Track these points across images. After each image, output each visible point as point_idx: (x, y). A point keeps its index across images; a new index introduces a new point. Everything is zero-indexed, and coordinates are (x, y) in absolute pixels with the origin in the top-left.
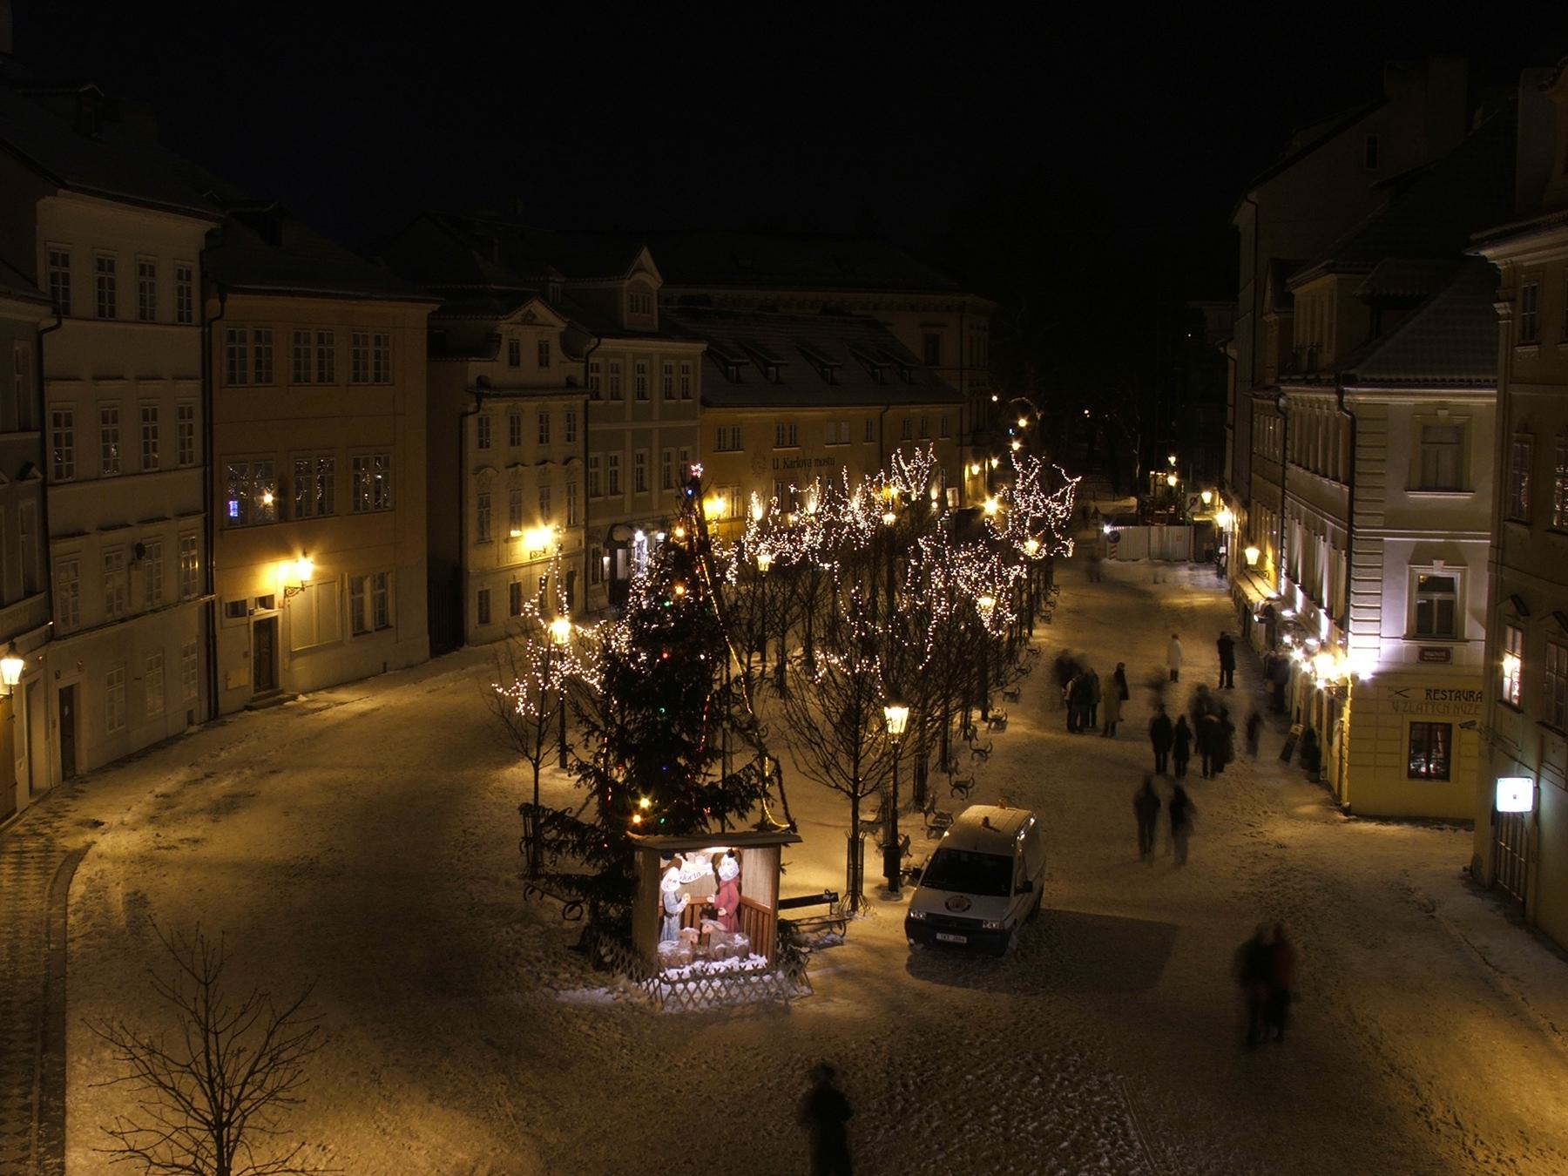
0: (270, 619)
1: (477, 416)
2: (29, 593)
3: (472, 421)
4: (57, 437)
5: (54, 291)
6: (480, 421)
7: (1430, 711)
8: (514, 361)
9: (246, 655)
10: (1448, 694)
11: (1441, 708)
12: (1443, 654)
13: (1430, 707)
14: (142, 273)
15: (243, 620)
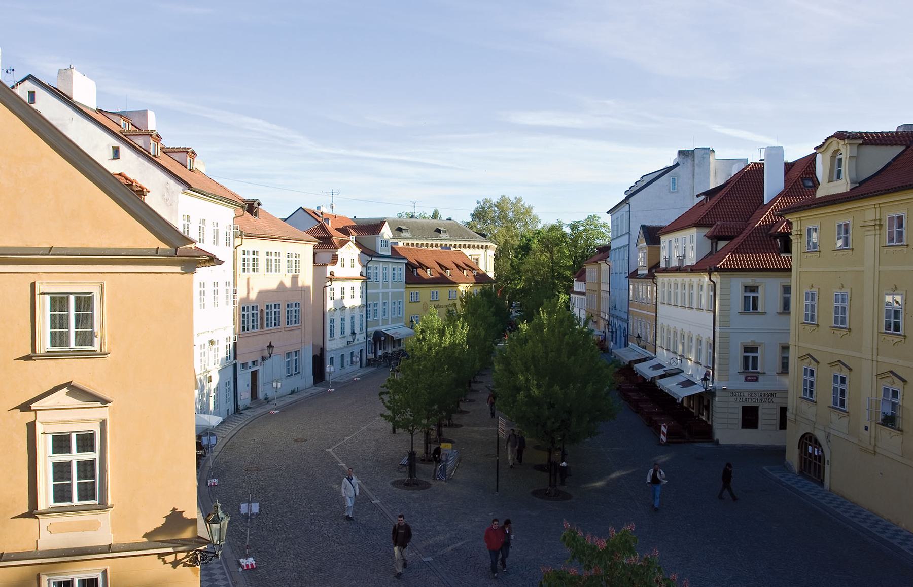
0: (256, 370)
1: (330, 287)
3: (328, 289)
7: (750, 401)
8: (343, 265)
9: (248, 385)
10: (757, 394)
11: (754, 400)
12: (755, 378)
13: (750, 400)
15: (247, 371)
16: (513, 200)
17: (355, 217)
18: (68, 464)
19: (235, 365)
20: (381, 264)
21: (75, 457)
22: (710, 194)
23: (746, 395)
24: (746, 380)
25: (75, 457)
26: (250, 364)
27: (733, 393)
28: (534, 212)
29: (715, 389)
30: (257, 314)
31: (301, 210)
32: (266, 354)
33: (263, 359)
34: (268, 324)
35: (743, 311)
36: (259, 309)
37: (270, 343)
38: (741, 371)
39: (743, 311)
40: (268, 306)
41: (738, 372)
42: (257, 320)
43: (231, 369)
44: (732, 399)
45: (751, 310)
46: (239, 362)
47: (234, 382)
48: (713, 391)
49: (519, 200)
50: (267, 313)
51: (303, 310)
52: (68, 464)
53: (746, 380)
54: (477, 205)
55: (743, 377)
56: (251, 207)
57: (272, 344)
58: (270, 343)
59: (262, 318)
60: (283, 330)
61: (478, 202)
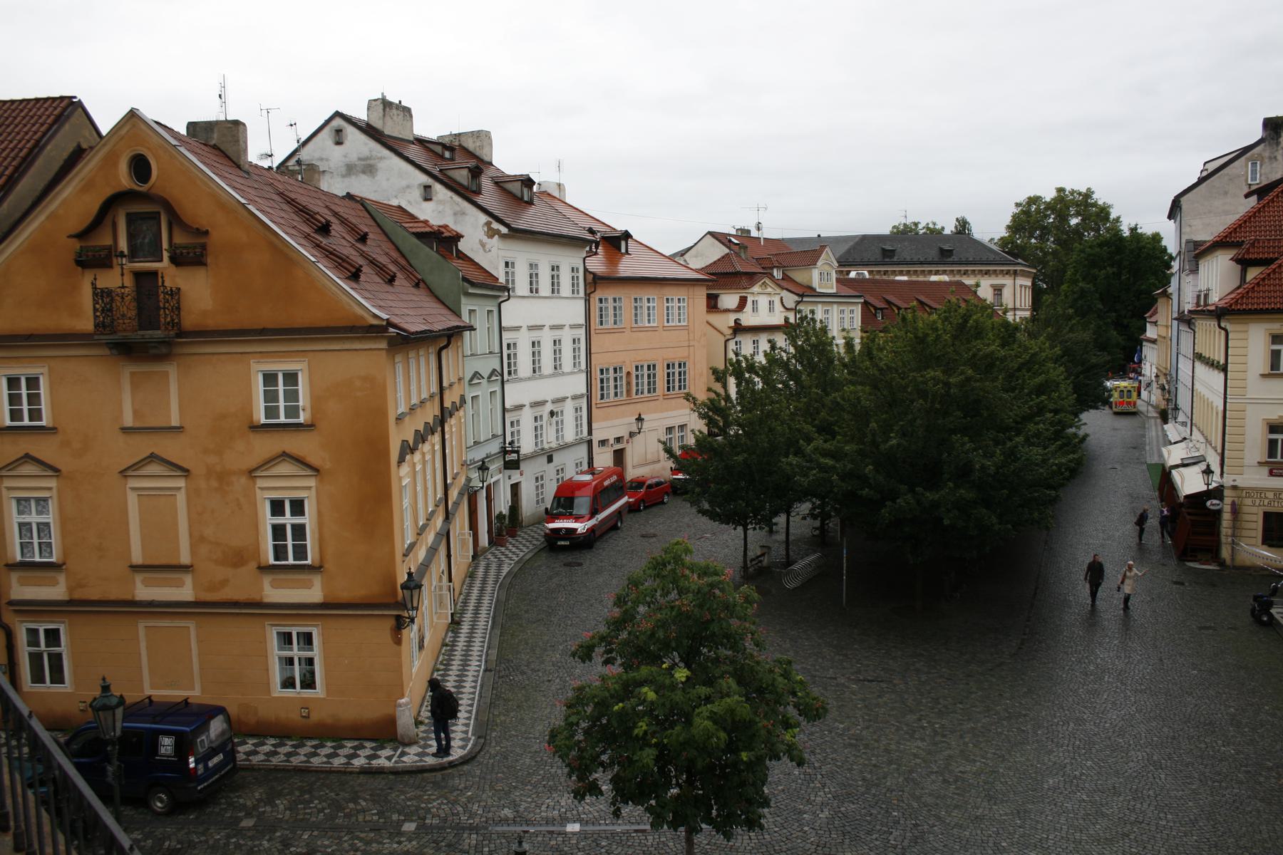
1: (735, 340)
2: (494, 436)
4: (509, 356)
5: (507, 281)
6: (736, 342)
8: (755, 309)
14: (553, 270)
17: (819, 236)
18: (283, 527)
19: (590, 443)
20: (820, 306)
21: (288, 519)
22: (1261, 192)
23: (1270, 495)
24: (1271, 474)
25: (288, 519)
26: (612, 441)
27: (1251, 491)
28: (1113, 216)
29: (1222, 486)
30: (621, 377)
31: (708, 236)
32: (635, 429)
33: (632, 435)
34: (637, 390)
35: (1268, 371)
36: (624, 371)
37: (640, 415)
39: (1268, 371)
40: (637, 367)
41: (1259, 463)
42: (621, 385)
43: (584, 448)
46: (597, 437)
47: (589, 463)
49: (1088, 194)
50: (637, 376)
51: (692, 373)
52: (283, 527)
53: (1271, 474)
55: (1265, 470)
56: (616, 242)
57: (642, 416)
58: (640, 415)
59: (629, 383)
60: (661, 398)
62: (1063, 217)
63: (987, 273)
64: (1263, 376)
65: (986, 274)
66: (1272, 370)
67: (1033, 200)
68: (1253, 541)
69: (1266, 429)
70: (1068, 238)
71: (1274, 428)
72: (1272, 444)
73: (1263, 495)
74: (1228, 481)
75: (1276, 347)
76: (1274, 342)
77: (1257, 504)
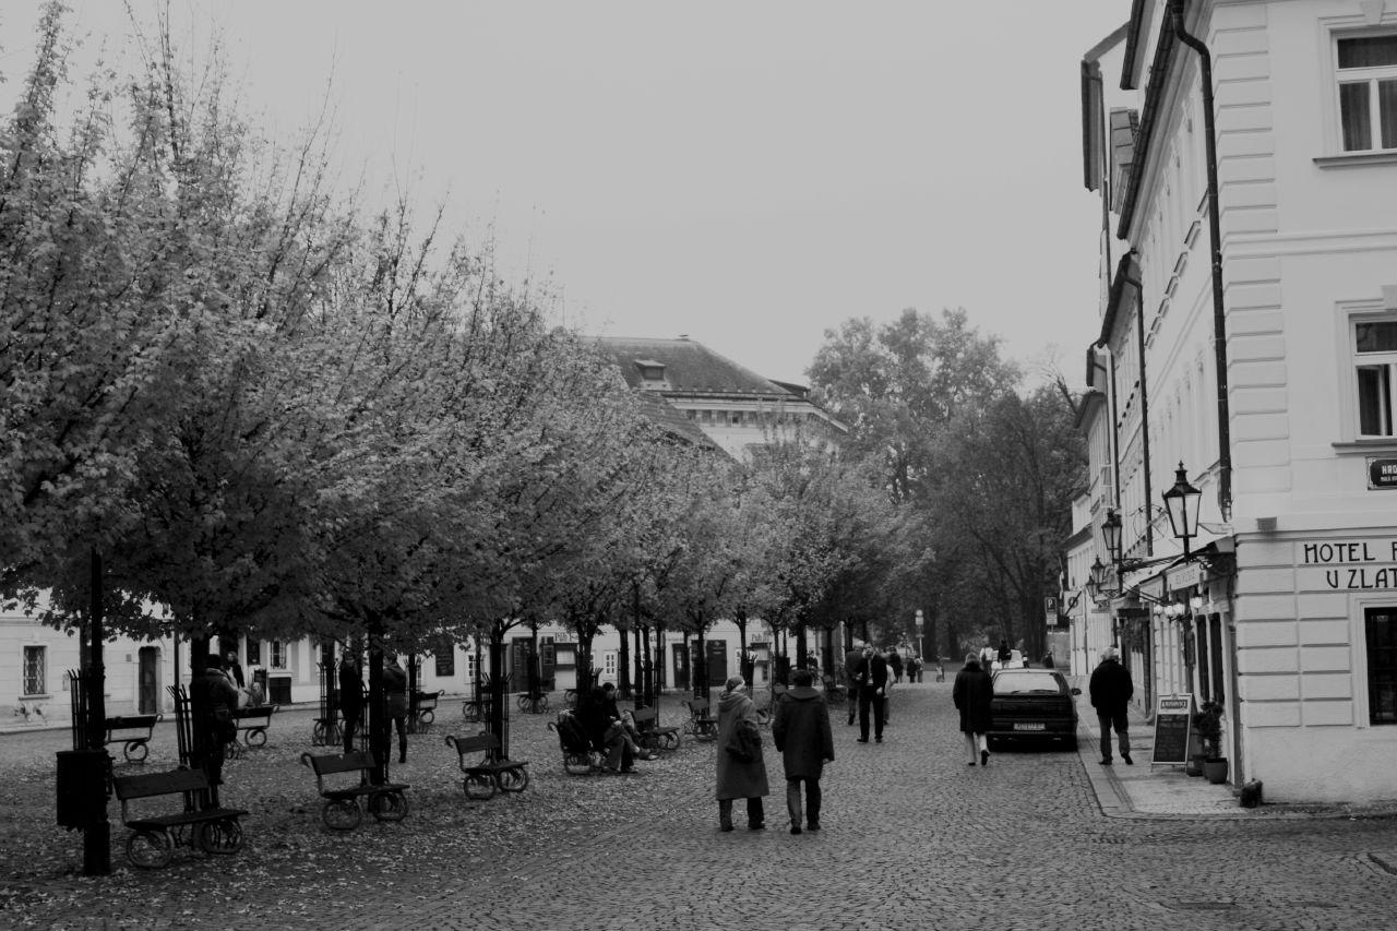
16: (942, 323)
24: (1377, 479)
28: (1004, 355)
38: (1351, 441)
39: (1337, 148)
41: (1335, 446)
44: (1316, 577)
45: (1377, 146)
48: (1222, 548)
54: (823, 341)
55: (1360, 468)
61: (829, 334)
62: (909, 351)
63: (737, 418)
64: (1325, 163)
65: (735, 420)
66: (1348, 147)
67: (858, 327)
68: (1340, 713)
69: (1350, 338)
70: (924, 400)
71: (1378, 332)
72: (1371, 382)
73: (1358, 553)
74: (1246, 514)
75: (1354, 75)
76: (1345, 61)
77: (1343, 584)
